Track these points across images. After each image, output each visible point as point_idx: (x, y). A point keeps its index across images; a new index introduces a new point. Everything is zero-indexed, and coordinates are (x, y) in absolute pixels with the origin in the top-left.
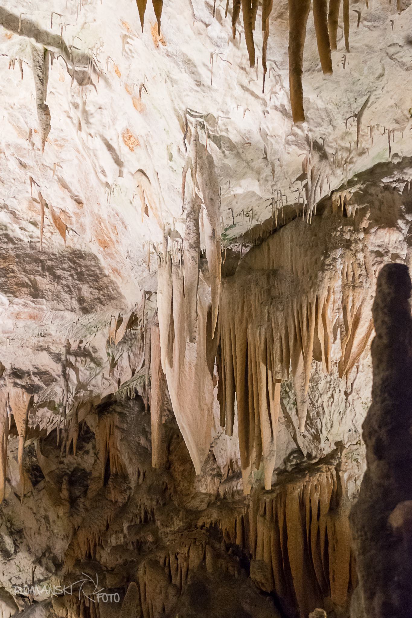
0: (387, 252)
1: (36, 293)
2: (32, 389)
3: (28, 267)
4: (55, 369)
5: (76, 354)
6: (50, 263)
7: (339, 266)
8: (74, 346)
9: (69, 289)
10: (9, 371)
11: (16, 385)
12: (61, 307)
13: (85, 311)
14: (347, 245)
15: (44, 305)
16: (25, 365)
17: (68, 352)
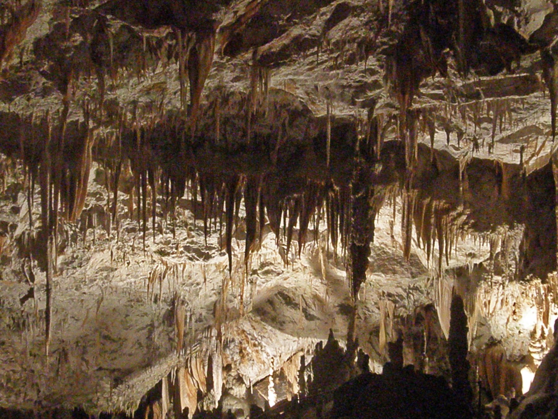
0: (498, 282)
1: (395, 272)
2: (395, 302)
3: (391, 263)
4: (405, 295)
5: (412, 289)
6: (400, 260)
7: (483, 285)
8: (412, 286)
9: (407, 270)
10: (386, 294)
11: (389, 300)
12: (404, 276)
13: (413, 277)
14: (485, 280)
15: (398, 276)
16: (393, 291)
17: (409, 288)
